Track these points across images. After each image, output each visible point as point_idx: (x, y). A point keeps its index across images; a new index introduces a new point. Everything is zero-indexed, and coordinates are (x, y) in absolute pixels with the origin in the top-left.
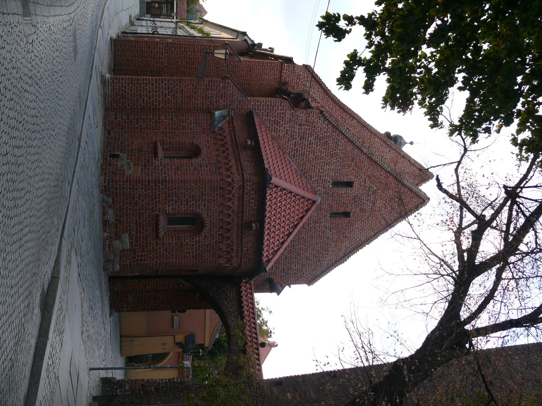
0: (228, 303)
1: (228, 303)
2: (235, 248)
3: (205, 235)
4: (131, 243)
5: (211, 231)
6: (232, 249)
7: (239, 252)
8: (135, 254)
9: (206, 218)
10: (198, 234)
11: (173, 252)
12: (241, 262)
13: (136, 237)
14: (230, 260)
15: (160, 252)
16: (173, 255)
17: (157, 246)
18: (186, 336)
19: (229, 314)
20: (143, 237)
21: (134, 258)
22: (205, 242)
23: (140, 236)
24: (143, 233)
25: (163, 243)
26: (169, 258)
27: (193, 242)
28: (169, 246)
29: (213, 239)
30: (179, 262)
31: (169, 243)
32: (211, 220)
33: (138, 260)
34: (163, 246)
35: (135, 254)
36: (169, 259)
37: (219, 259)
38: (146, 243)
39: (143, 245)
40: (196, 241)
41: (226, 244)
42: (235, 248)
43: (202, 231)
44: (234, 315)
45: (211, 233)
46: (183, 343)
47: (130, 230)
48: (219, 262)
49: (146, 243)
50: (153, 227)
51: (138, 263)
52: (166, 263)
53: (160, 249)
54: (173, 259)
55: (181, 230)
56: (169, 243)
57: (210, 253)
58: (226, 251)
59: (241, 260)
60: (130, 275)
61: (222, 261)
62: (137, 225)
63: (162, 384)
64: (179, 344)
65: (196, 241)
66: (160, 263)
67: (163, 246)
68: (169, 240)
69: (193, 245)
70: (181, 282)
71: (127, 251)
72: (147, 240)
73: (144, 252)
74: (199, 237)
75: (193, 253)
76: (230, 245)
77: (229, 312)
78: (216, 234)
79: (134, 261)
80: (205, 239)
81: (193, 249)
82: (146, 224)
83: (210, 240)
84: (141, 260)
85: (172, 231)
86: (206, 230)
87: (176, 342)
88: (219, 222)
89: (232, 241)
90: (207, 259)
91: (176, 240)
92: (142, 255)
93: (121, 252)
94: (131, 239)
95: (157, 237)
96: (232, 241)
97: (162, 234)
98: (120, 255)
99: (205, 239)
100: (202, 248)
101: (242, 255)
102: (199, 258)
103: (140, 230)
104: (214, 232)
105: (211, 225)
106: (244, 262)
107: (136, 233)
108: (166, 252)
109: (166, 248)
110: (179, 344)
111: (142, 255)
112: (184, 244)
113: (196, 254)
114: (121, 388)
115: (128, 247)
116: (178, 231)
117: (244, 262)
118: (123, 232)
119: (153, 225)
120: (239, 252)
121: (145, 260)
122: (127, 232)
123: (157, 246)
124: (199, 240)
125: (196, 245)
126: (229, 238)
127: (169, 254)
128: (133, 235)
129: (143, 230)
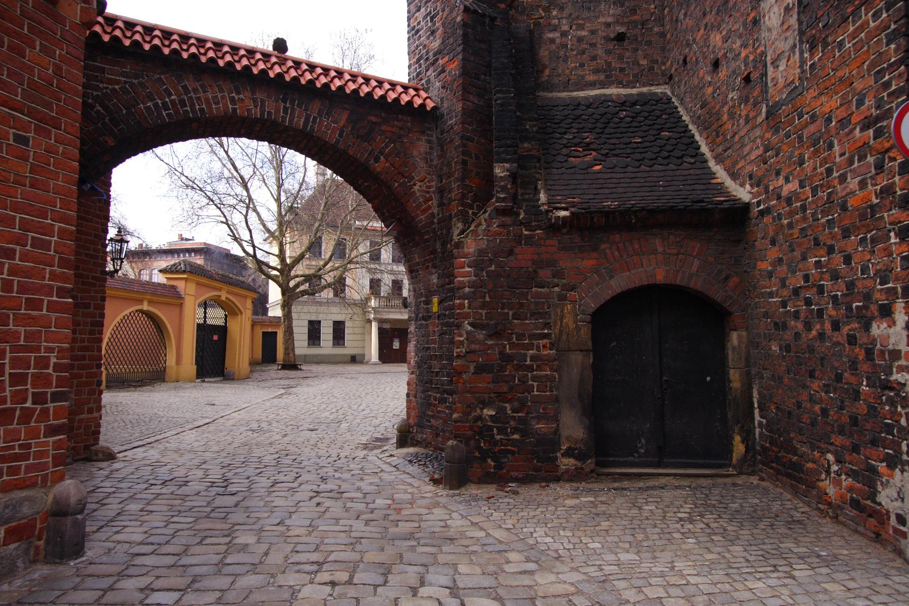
1: (151, 98)
19: (192, 106)
21: (27, 416)
26: (36, 243)
33: (39, 399)
36: (46, 245)
44: (195, 91)
51: (56, 397)
52: (63, 263)
66: (62, 292)
84: (41, 380)
102: (48, 105)
111: (17, 379)
114: (490, 429)
121: (43, 363)
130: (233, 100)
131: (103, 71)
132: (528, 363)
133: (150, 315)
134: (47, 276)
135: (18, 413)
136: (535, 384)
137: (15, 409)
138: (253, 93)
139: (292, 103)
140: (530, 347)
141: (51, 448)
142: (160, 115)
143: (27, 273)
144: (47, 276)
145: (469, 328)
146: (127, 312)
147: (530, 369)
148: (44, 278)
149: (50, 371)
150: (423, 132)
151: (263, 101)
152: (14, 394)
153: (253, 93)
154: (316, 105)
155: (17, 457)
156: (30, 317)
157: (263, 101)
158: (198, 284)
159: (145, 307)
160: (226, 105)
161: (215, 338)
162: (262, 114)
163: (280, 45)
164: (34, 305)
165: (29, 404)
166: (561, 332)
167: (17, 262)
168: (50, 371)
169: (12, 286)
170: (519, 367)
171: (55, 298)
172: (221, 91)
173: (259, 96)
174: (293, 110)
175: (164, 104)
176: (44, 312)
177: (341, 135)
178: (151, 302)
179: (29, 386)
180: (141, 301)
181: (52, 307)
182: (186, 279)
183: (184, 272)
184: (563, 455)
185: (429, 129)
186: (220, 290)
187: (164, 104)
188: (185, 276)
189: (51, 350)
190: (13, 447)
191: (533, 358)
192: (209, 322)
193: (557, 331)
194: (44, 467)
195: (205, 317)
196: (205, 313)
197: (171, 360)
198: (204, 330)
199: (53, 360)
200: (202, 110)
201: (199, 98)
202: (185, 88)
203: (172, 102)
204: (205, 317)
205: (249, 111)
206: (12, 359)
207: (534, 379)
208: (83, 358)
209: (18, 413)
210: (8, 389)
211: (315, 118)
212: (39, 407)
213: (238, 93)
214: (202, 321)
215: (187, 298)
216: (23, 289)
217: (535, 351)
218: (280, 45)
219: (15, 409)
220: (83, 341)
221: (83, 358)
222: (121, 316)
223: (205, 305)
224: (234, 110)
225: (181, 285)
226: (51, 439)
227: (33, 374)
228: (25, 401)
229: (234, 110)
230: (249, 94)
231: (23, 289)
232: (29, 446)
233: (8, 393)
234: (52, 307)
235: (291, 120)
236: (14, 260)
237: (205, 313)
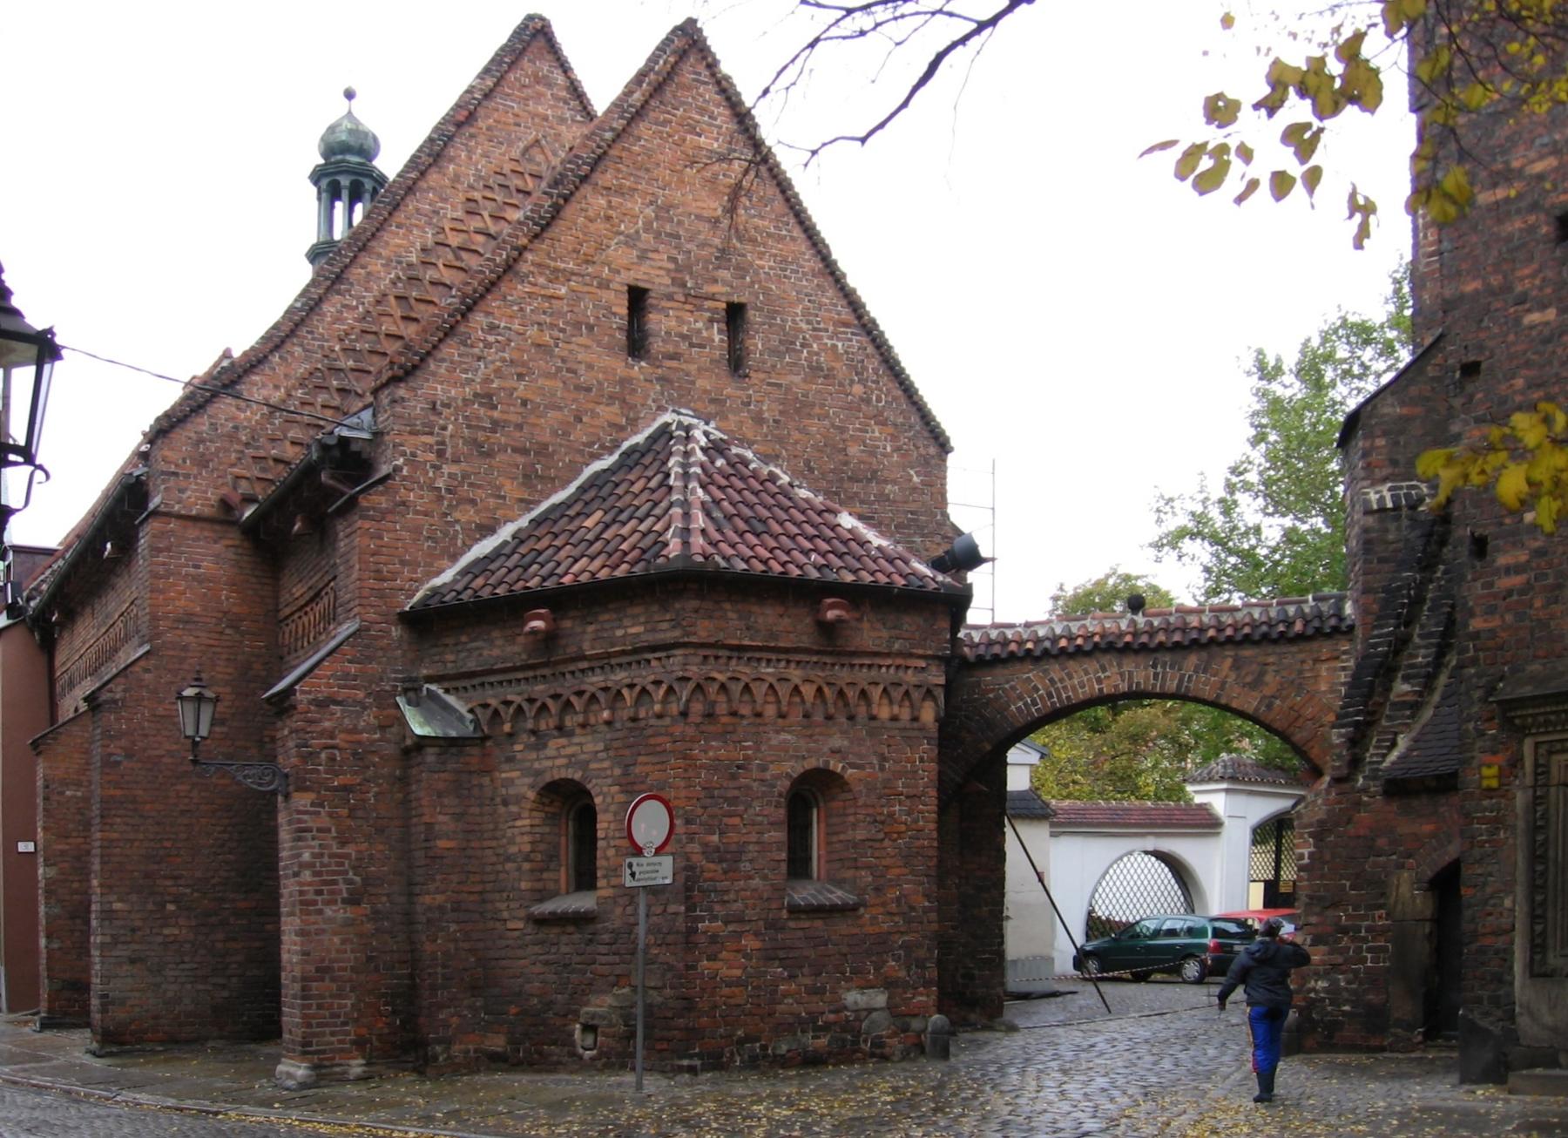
0: (1021, 698)
1: (1021, 698)
19: (1059, 696)
44: (1061, 680)
77: (1050, 696)
130: (1099, 681)
138: (1120, 666)
139: (1164, 667)
153: (1120, 666)
160: (1092, 687)
162: (1130, 686)
174: (1164, 673)
200: (1068, 698)
201: (1065, 688)
202: (1052, 681)
203: (1041, 697)
205: (1116, 687)
224: (1101, 690)
229: (1101, 690)
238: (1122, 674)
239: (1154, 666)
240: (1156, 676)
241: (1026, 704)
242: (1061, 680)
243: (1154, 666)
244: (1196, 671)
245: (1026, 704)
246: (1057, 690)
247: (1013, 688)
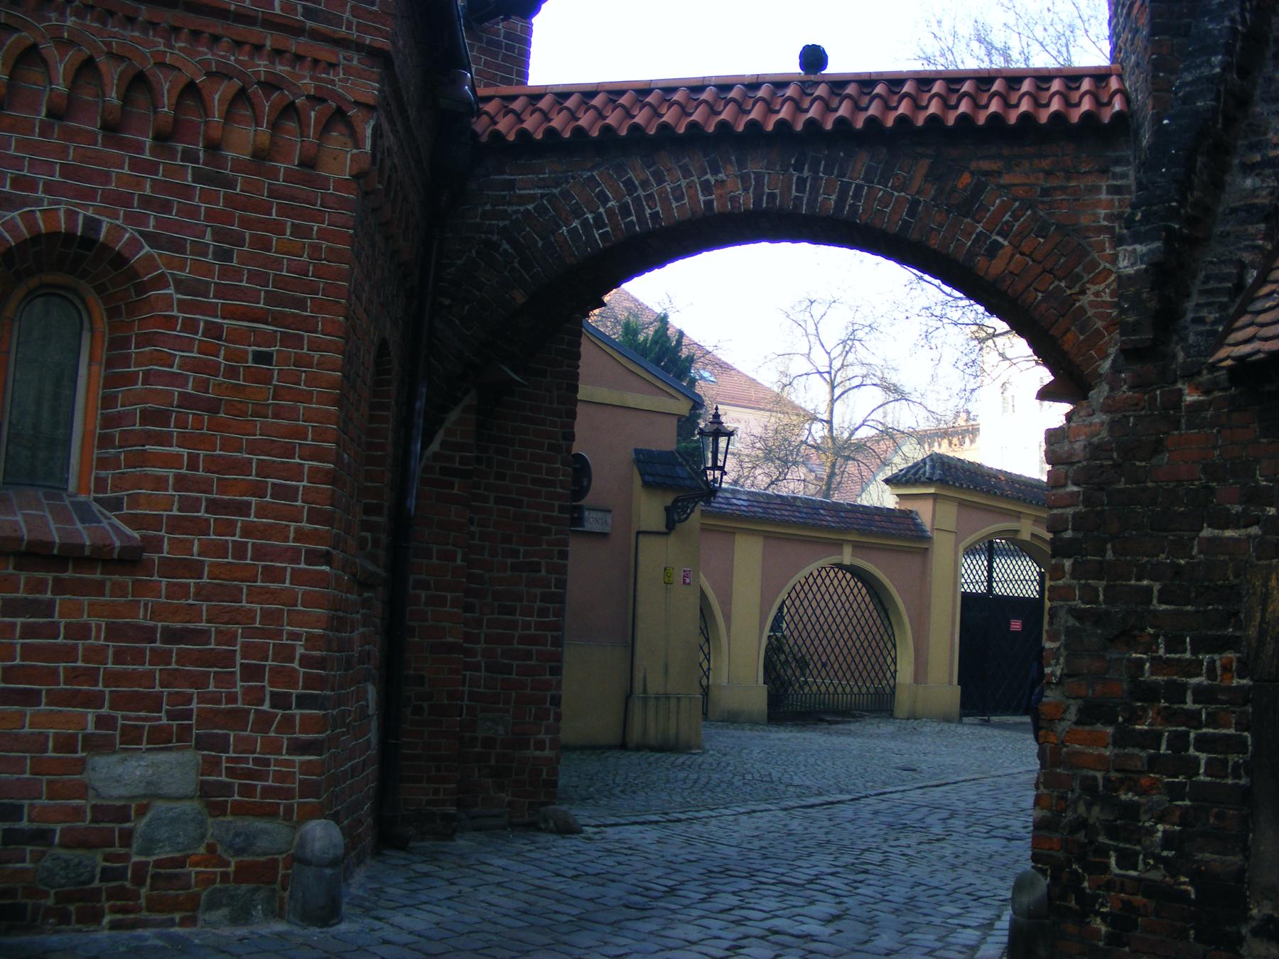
0: (577, 213)
1: (577, 213)
2: (262, 66)
3: (152, 239)
4: (160, 739)
5: (126, 201)
6: (271, 85)
7: (293, 45)
8: (237, 718)
9: (29, 218)
10: (142, 288)
11: (244, 467)
12: (359, 47)
13: (119, 702)
14: (340, 113)
15: (240, 550)
16: (264, 469)
17: (194, 569)
18: (646, 484)
20: (119, 657)
21: (264, 722)
22: (201, 250)
23: (112, 678)
24: (95, 654)
25: (176, 525)
26: (279, 492)
27: (190, 326)
28: (205, 486)
29: (186, 192)
30: (318, 434)
31: (181, 483)
32: (49, 188)
33: (280, 701)
34: (200, 527)
35: (237, 718)
36: (290, 493)
37: (324, 182)
38: (172, 636)
39: (183, 658)
40: (183, 306)
41: (229, 116)
42: (262, 66)
43: (120, 260)
44: (645, 184)
45: (146, 202)
46: (669, 499)
47: (66, 744)
48: (340, 184)
49: (172, 636)
50: (60, 587)
51: (303, 702)
52: (314, 517)
53: (221, 550)
54: (296, 473)
55: (108, 401)
56: (181, 483)
57: (279, 228)
58: (274, 126)
59: (342, 43)
60: (373, 736)
61: (343, 159)
62: (31, 698)
63: (1089, 594)
64: (673, 518)
65: (183, 306)
66: (313, 557)
67: (200, 527)
68: (160, 483)
69: (213, 331)
70: (436, 456)
71: (211, 765)
72: (148, 634)
73: (228, 659)
74: (160, 282)
75: (269, 340)
76: (242, 91)
78: (151, 168)
79: (287, 723)
80: (178, 246)
81: (236, 336)
82: (28, 631)
83: (194, 213)
84: (287, 677)
85: (103, 463)
86: (117, 231)
87: (663, 529)
88: (70, 135)
89: (220, 74)
90: (315, 249)
91: (164, 440)
92: (251, 673)
93: (217, 809)
94: (131, 736)
95: (130, 560)
96: (220, 74)
97: (116, 530)
98: (240, 810)
99: (178, 246)
100: (237, 273)
101: (315, 35)
102: (301, 304)
103: (73, 675)
104: (139, 183)
105: (91, 195)
106: (362, 29)
107: (93, 700)
108: (243, 509)
109: (213, 506)
110: (673, 518)
111: (251, 673)
112: (204, 386)
113: (277, 320)
114: (1103, 851)
115: (191, 757)
116: (108, 422)
117: (362, 29)
118: (82, 790)
119: (40, 586)
120: (293, 45)
121: (285, 653)
122: (81, 765)
123: (194, 569)
124: (180, 285)
125: (210, 310)
126: (191, 89)
127: (258, 490)
128: (101, 721)
129: (70, 654)
130: (707, 187)
131: (511, 185)
132: (1189, 705)
133: (856, 572)
134: (292, 535)
135: (252, 717)
136: (1203, 757)
137: (248, 711)
138: (741, 164)
139: (814, 170)
140: (1192, 668)
141: (296, 770)
142: (591, 240)
143: (265, 532)
144: (292, 535)
145: (1071, 622)
146: (813, 567)
147: (1192, 719)
148: (286, 539)
149: (296, 665)
150: (1104, 171)
151: (759, 177)
152: (247, 691)
153: (741, 164)
154: (862, 162)
155: (250, 774)
156: (273, 592)
157: (759, 177)
158: (962, 504)
159: (847, 557)
160: (694, 199)
161: (1016, 625)
163: (813, 57)
164: (273, 575)
165: (266, 707)
166: (1262, 633)
167: (252, 518)
168: (296, 665)
169: (246, 551)
170: (1170, 716)
171: (303, 566)
172: (687, 173)
173: (753, 168)
174: (816, 179)
175: (598, 218)
176: (287, 585)
177: (912, 213)
178: (857, 546)
179: (266, 683)
180: (839, 545)
181: (298, 577)
182: (934, 496)
183: (929, 482)
184: (1256, 932)
185: (1118, 162)
186: (1018, 516)
187: (598, 218)
188: (932, 490)
189: (296, 636)
190: (246, 760)
191: (1202, 695)
192: (998, 589)
193: (1252, 632)
194: (288, 794)
195: (990, 579)
196: (990, 569)
197: (905, 671)
198: (981, 612)
199: (300, 651)
200: (655, 216)
201: (650, 197)
202: (629, 184)
203: (610, 212)
204: (990, 579)
205: (734, 200)
206: (244, 645)
207: (1202, 743)
208: (528, 655)
209: (252, 717)
210: (239, 684)
211: (859, 188)
212: (280, 712)
213: (715, 171)
214: (982, 589)
215: (937, 536)
216: (259, 554)
217: (1202, 680)
218: (813, 57)
219: (248, 711)
220: (527, 626)
221: (528, 655)
222: (806, 572)
223: (991, 552)
224: (709, 204)
225: (925, 512)
226: (297, 758)
227: (271, 668)
228: (262, 702)
229: (709, 204)
230: (733, 169)
231: (259, 554)
232: (266, 763)
233: (238, 689)
234: (298, 577)
235: (812, 201)
236: (249, 516)
237: (990, 569)
238: (744, 179)
239: (798, 167)
240: (801, 182)
241: (585, 224)
242: (645, 184)
243: (798, 167)
244: (868, 179)
245: (585, 224)
246: (637, 200)
247: (566, 195)
